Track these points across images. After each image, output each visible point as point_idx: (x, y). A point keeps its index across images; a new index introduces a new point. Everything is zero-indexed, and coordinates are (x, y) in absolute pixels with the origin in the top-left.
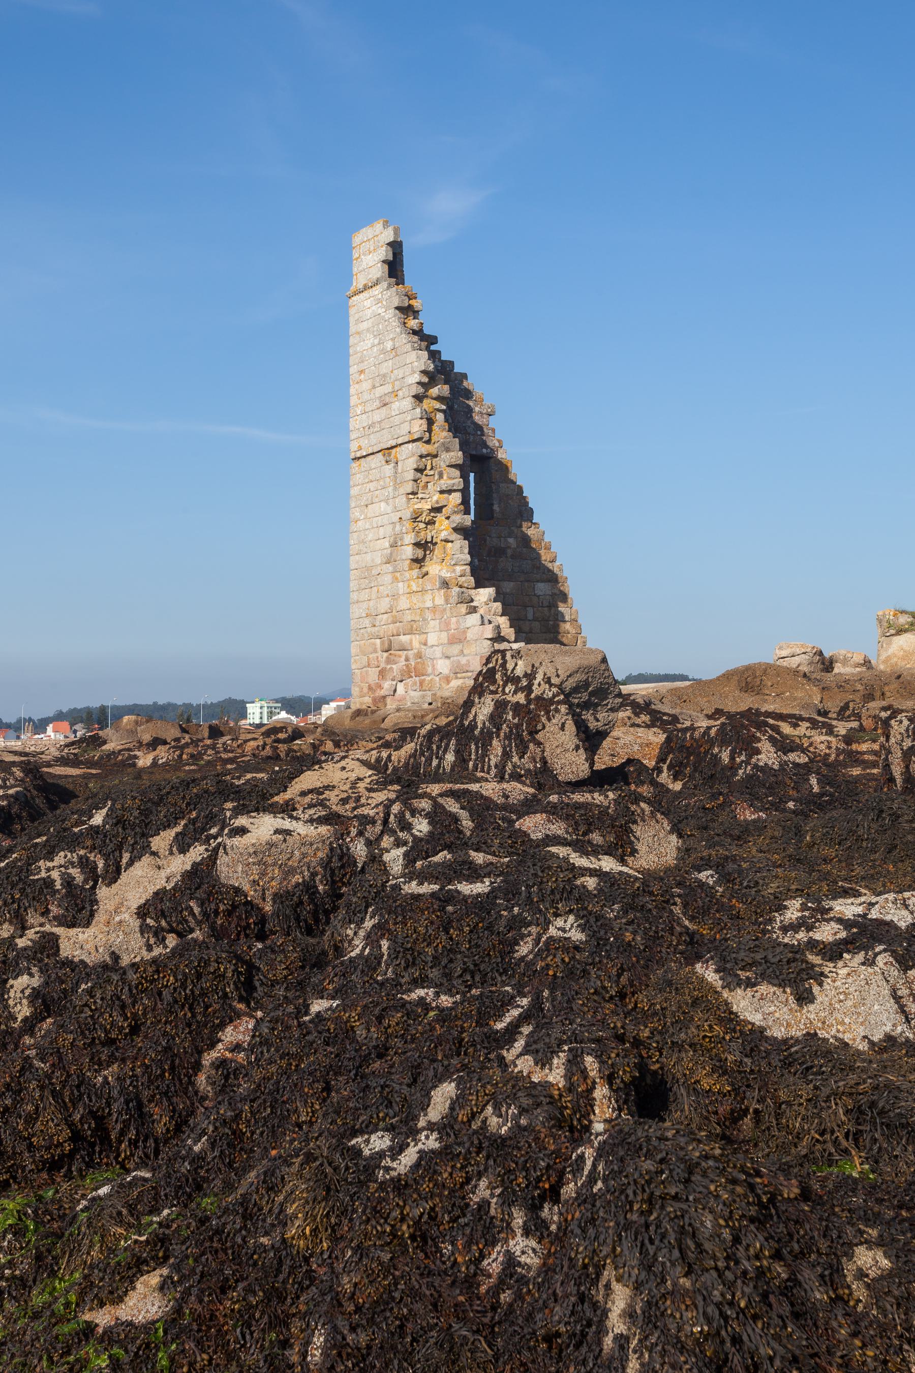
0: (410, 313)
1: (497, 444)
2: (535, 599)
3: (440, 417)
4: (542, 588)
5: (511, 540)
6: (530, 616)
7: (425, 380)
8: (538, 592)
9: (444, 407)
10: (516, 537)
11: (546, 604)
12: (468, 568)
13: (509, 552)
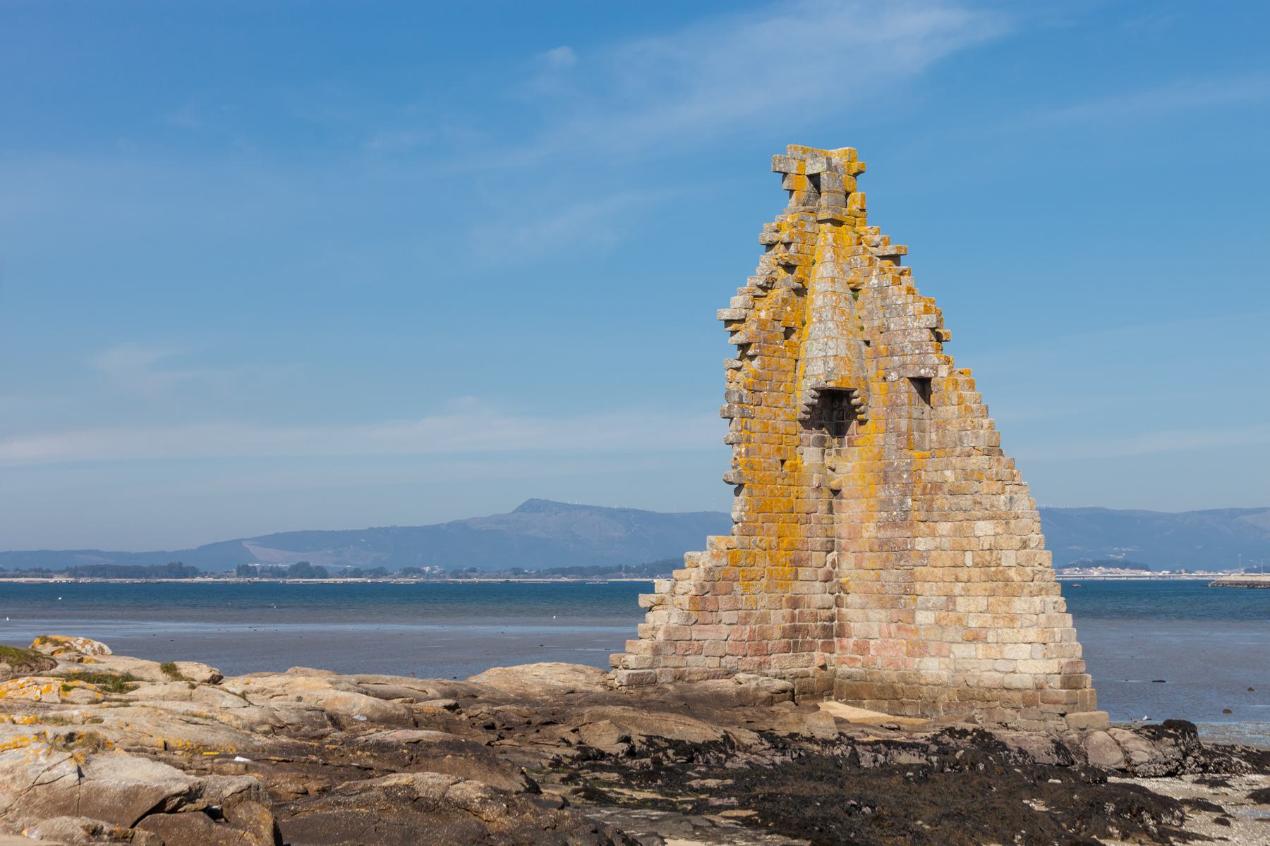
5: (948, 473)
6: (969, 562)
11: (986, 546)
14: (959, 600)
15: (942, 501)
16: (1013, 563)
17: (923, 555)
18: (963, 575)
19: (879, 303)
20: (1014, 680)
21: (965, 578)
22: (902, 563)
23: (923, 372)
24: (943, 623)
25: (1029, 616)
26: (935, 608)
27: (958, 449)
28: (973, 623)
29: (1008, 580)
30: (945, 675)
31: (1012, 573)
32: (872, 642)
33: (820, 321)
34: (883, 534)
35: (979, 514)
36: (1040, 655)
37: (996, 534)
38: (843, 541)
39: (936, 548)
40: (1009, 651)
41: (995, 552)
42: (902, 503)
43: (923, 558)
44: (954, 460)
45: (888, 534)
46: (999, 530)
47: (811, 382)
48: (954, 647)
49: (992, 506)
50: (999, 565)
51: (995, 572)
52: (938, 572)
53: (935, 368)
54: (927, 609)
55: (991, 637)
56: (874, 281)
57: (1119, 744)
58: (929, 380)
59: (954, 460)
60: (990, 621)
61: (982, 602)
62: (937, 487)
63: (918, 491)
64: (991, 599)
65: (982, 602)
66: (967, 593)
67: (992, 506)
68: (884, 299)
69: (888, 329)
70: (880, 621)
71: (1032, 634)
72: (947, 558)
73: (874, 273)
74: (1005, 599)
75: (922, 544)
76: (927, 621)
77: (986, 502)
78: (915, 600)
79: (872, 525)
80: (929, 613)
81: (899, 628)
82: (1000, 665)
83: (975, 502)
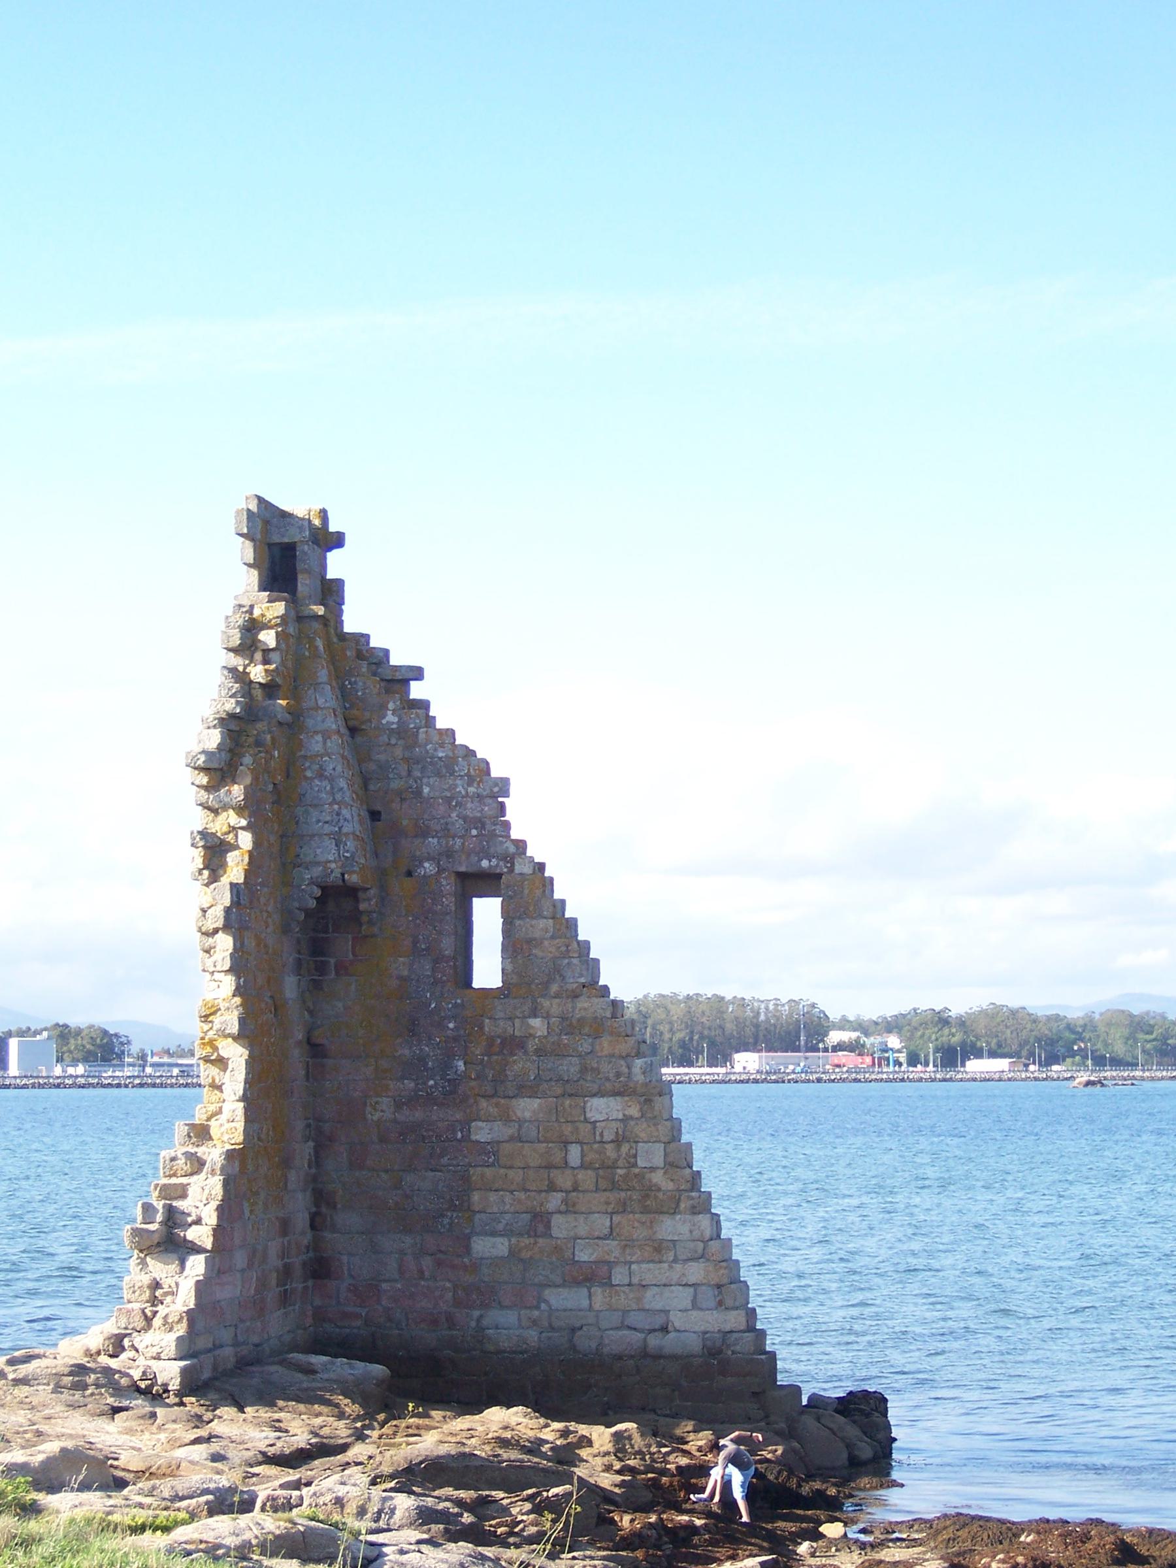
0: (258, 656)
1: (512, 849)
2: (585, 1129)
3: (246, 840)
4: (603, 1109)
5: (536, 1022)
7: (204, 780)
8: (592, 1115)
9: (244, 823)
10: (547, 1016)
11: (608, 1136)
12: (242, 1104)
13: (531, 1046)
14: (557, 1220)
15: (520, 1065)
16: (658, 1160)
17: (490, 1151)
18: (564, 1180)
19: (398, 752)
20: (668, 1343)
21: (568, 1185)
22: (445, 1160)
23: (485, 863)
24: (525, 1255)
25: (691, 1245)
26: (507, 1233)
27: (554, 988)
28: (583, 1256)
29: (650, 1190)
30: (532, 1335)
31: (658, 1178)
32: (384, 1286)
33: (321, 775)
34: (405, 1116)
35: (595, 1088)
36: (712, 1304)
37: (626, 1119)
38: (327, 1127)
39: (511, 1139)
40: (653, 1299)
41: (625, 1148)
42: (446, 1065)
43: (488, 1154)
44: (546, 1003)
45: (419, 1115)
46: (634, 1111)
47: (317, 871)
48: (547, 1293)
49: (618, 1075)
50: (635, 1165)
51: (626, 1176)
52: (516, 1176)
53: (509, 859)
54: (493, 1234)
55: (619, 1276)
56: (390, 718)
57: (834, 1434)
58: (499, 876)
59: (546, 1003)
60: (617, 1253)
61: (602, 1223)
62: (513, 1044)
63: (477, 1051)
64: (616, 1218)
65: (602, 1223)
66: (569, 1208)
67: (618, 1075)
68: (407, 748)
69: (418, 793)
70: (402, 1252)
71: (696, 1272)
72: (533, 1155)
73: (391, 706)
74: (644, 1218)
75: (482, 1132)
76: (495, 1252)
77: (606, 1068)
78: (470, 1220)
79: (385, 1102)
80: (499, 1240)
81: (439, 1264)
82: (635, 1319)
83: (584, 1070)
